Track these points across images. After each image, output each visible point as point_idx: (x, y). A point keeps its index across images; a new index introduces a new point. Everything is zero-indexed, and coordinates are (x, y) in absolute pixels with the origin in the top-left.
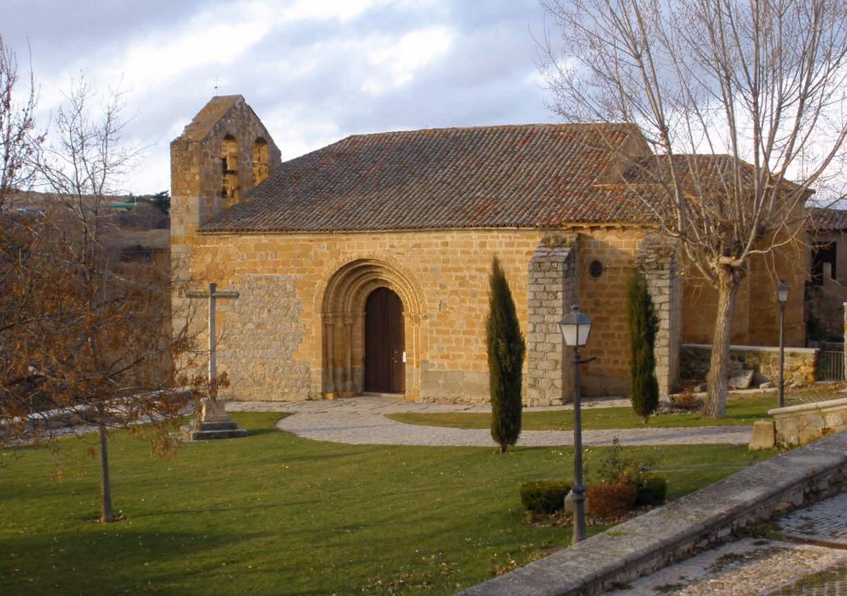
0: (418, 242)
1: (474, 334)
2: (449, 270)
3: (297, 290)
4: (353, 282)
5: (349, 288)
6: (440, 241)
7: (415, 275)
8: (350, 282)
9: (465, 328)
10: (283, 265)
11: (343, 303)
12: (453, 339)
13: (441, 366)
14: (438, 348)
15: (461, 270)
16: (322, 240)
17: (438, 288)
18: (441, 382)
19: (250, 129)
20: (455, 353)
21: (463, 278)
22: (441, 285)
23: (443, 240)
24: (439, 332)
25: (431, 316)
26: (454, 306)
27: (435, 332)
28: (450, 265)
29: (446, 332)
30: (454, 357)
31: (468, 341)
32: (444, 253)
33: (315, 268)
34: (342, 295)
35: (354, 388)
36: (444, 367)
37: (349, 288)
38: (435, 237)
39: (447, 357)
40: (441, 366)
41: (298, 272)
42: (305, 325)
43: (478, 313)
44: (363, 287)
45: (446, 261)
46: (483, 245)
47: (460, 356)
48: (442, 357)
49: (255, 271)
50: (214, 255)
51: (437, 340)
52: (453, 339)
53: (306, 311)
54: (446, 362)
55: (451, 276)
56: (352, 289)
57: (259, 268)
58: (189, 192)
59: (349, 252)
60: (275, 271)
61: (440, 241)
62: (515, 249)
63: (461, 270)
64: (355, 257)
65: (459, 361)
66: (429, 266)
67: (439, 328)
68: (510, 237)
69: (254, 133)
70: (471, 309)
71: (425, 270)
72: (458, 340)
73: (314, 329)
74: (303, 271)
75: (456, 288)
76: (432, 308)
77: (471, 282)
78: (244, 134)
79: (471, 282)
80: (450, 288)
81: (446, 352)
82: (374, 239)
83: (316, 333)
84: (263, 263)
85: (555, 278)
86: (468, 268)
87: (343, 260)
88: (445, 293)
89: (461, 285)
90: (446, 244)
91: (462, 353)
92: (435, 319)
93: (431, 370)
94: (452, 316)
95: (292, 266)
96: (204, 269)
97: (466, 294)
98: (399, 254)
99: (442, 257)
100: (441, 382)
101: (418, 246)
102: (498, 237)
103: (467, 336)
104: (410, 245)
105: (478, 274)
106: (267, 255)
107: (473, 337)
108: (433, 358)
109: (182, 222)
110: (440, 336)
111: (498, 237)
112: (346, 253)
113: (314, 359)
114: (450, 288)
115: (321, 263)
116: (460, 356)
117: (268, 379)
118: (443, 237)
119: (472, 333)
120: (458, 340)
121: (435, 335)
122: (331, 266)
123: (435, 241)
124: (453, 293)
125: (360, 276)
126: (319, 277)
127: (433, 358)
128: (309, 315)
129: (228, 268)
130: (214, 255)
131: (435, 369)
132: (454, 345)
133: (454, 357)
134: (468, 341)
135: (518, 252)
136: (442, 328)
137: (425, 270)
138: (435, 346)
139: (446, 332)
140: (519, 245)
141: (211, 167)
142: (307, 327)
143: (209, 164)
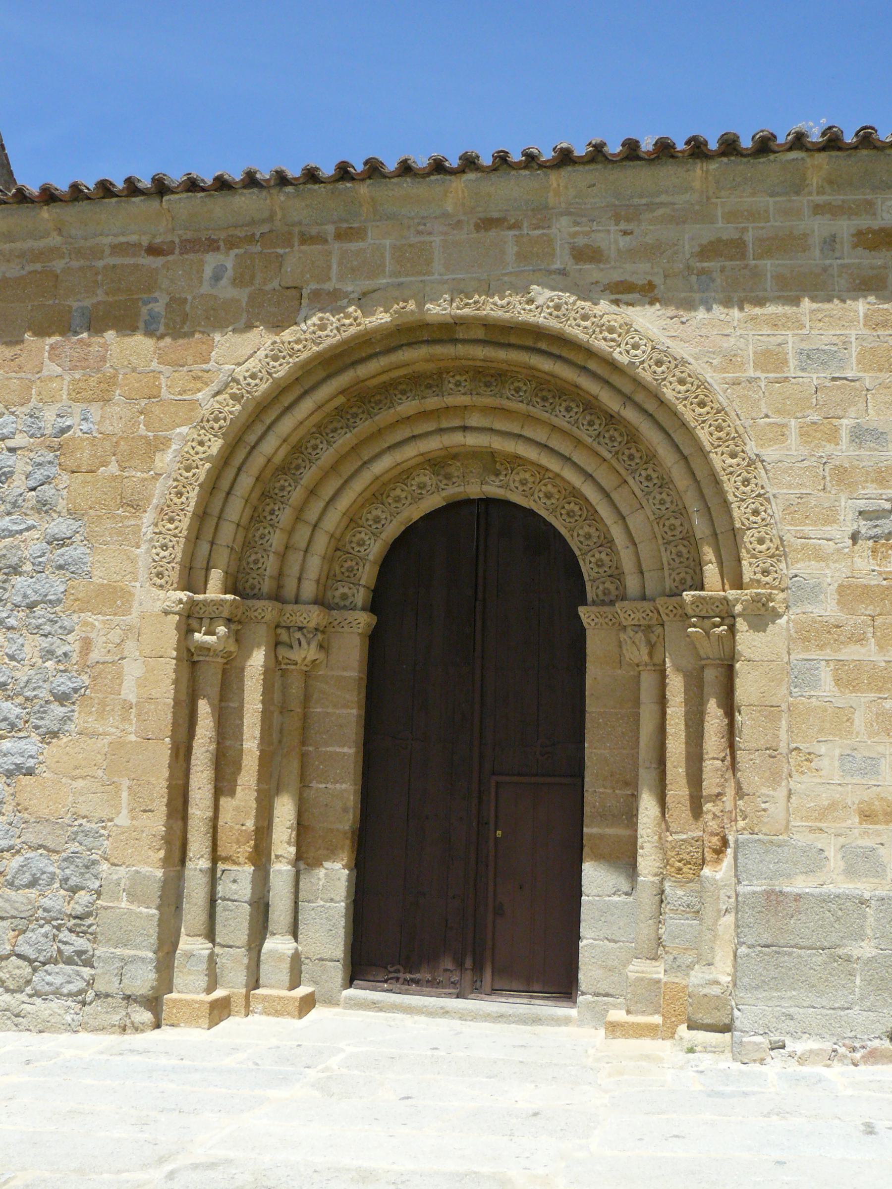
0: (725, 230)
4: (334, 468)
5: (312, 492)
6: (845, 227)
11: (283, 557)
22: (859, 435)
25: (814, 592)
27: (826, 675)
34: (285, 516)
37: (312, 492)
41: (77, 395)
42: (87, 644)
51: (841, 720)
56: (328, 491)
61: (845, 227)
67: (851, 653)
73: (133, 670)
83: (141, 683)
92: (828, 609)
113: (123, 820)
118: (869, 207)
123: (819, 227)
125: (380, 432)
128: (113, 598)
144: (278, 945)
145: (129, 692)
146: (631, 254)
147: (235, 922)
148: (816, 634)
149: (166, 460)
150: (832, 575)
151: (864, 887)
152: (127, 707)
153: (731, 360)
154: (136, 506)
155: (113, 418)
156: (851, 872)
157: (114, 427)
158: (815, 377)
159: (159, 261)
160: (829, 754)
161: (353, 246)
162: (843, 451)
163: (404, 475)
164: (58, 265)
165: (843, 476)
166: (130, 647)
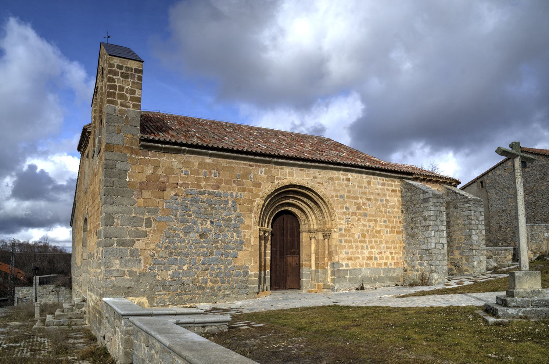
1: (366, 243)
3: (238, 206)
9: (361, 238)
10: (226, 183)
12: (354, 246)
13: (347, 265)
14: (345, 252)
15: (357, 198)
16: (260, 166)
17: (345, 210)
18: (348, 277)
21: (358, 204)
23: (347, 177)
24: (345, 242)
26: (354, 223)
28: (351, 195)
29: (349, 241)
31: (362, 247)
33: (254, 188)
36: (349, 266)
38: (342, 174)
40: (347, 265)
41: (239, 190)
42: (245, 235)
43: (368, 228)
46: (369, 183)
47: (358, 258)
48: (348, 259)
49: (199, 186)
50: (156, 168)
51: (344, 247)
52: (354, 246)
53: (245, 223)
54: (350, 262)
55: (352, 202)
57: (203, 184)
59: (283, 178)
60: (218, 188)
62: (386, 187)
64: (286, 182)
65: (357, 261)
67: (346, 238)
68: (383, 180)
70: (364, 226)
72: (357, 247)
73: (252, 240)
74: (244, 190)
75: (355, 210)
76: (341, 224)
77: (363, 207)
79: (363, 207)
80: (351, 211)
81: (350, 255)
82: (301, 170)
84: (207, 180)
85: (442, 203)
86: (361, 198)
87: (277, 184)
88: (349, 214)
89: (358, 208)
90: (348, 180)
91: (360, 256)
92: (343, 232)
94: (353, 231)
95: (234, 185)
96: (144, 179)
98: (319, 183)
99: (347, 189)
100: (348, 277)
101: (330, 179)
102: (377, 179)
104: (327, 178)
105: (367, 201)
106: (211, 172)
107: (365, 245)
108: (343, 259)
110: (347, 245)
111: (377, 179)
112: (280, 179)
113: (252, 264)
115: (259, 185)
116: (358, 258)
117: (210, 284)
119: (364, 242)
120: (357, 247)
121: (343, 244)
122: (268, 189)
124: (354, 214)
126: (258, 196)
127: (343, 259)
128: (248, 227)
129: (171, 181)
130: (156, 168)
131: (344, 268)
132: (355, 250)
134: (362, 247)
135: (387, 190)
136: (347, 238)
137: (337, 196)
138: (343, 251)
139: (349, 241)
140: (388, 185)
142: (246, 237)
145: (252, 243)
146: (321, 178)
149: (255, 204)
152: (252, 246)
153: (332, 196)
154: (251, 211)
155: (245, 195)
156: (346, 267)
157: (246, 197)
158: (342, 199)
159: (251, 168)
161: (283, 171)
164: (233, 166)
165: (345, 213)
166: (252, 236)
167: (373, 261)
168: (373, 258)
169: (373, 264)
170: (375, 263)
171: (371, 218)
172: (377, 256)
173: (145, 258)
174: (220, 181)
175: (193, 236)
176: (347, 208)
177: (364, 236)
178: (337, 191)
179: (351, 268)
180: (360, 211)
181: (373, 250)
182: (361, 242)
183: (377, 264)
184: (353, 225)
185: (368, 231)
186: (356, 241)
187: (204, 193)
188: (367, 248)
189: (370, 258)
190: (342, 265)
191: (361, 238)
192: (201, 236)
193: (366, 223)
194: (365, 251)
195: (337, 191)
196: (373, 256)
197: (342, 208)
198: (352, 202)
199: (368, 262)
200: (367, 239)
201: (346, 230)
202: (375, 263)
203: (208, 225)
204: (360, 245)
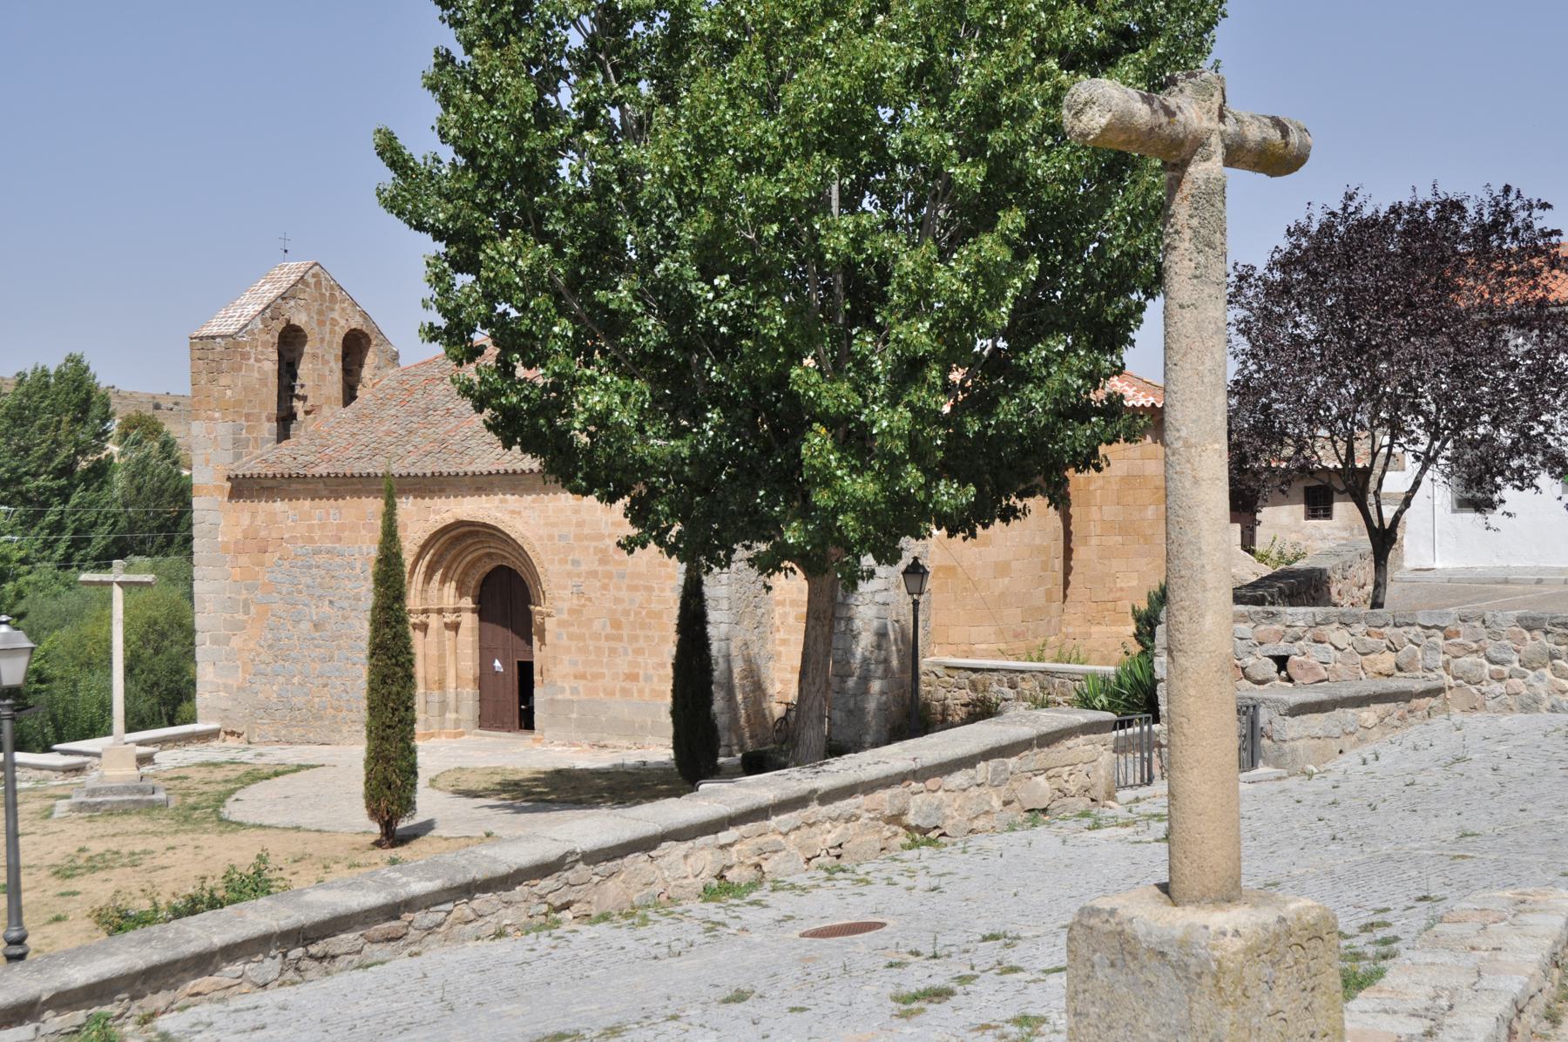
2: (586, 537)
7: (537, 544)
8: (449, 557)
9: (609, 630)
17: (569, 567)
18: (574, 716)
19: (335, 315)
20: (594, 670)
25: (560, 611)
28: (586, 531)
29: (581, 637)
30: (596, 676)
32: (577, 512)
35: (457, 723)
39: (582, 676)
44: (472, 564)
45: (580, 524)
47: (602, 676)
48: (576, 677)
49: (311, 540)
54: (581, 684)
55: (587, 548)
57: (317, 535)
58: (217, 415)
63: (600, 537)
66: (556, 532)
67: (571, 629)
69: (343, 322)
70: (617, 600)
71: (551, 538)
72: (599, 650)
78: (321, 323)
81: (580, 668)
88: (579, 575)
89: (603, 561)
92: (565, 616)
93: (560, 697)
95: (363, 532)
96: (240, 536)
97: (609, 575)
98: (513, 512)
100: (574, 716)
103: (613, 644)
108: (564, 677)
109: (207, 462)
114: (584, 568)
116: (602, 676)
119: (619, 638)
120: (599, 650)
121: (565, 641)
124: (594, 574)
131: (568, 695)
132: (592, 657)
133: (596, 676)
134: (613, 651)
136: (575, 629)
137: (551, 538)
141: (256, 374)
143: (251, 369)
144: (451, 716)
147: (434, 709)
148: (561, 624)
150: (566, 606)
151: (575, 698)
153: (541, 538)
158: (562, 543)
160: (566, 658)
162: (569, 567)
163: (479, 559)
165: (569, 574)
167: (642, 683)
168: (641, 678)
169: (641, 691)
170: (647, 691)
171: (636, 582)
172: (651, 672)
173: (244, 663)
174: (341, 528)
175: (305, 626)
176: (576, 563)
177: (616, 625)
178: (554, 525)
179: (583, 697)
180: (608, 568)
181: (640, 659)
182: (608, 638)
183: (652, 690)
184: (589, 599)
185: (627, 613)
186: (596, 637)
187: (317, 552)
188: (626, 653)
189: (633, 677)
190: (563, 690)
191: (609, 630)
192: (316, 626)
193: (624, 594)
194: (617, 660)
195: (554, 525)
196: (641, 673)
197: (563, 561)
198: (587, 548)
199: (628, 685)
200: (625, 633)
201: (571, 611)
202: (647, 691)
203: (326, 607)
204: (605, 645)
